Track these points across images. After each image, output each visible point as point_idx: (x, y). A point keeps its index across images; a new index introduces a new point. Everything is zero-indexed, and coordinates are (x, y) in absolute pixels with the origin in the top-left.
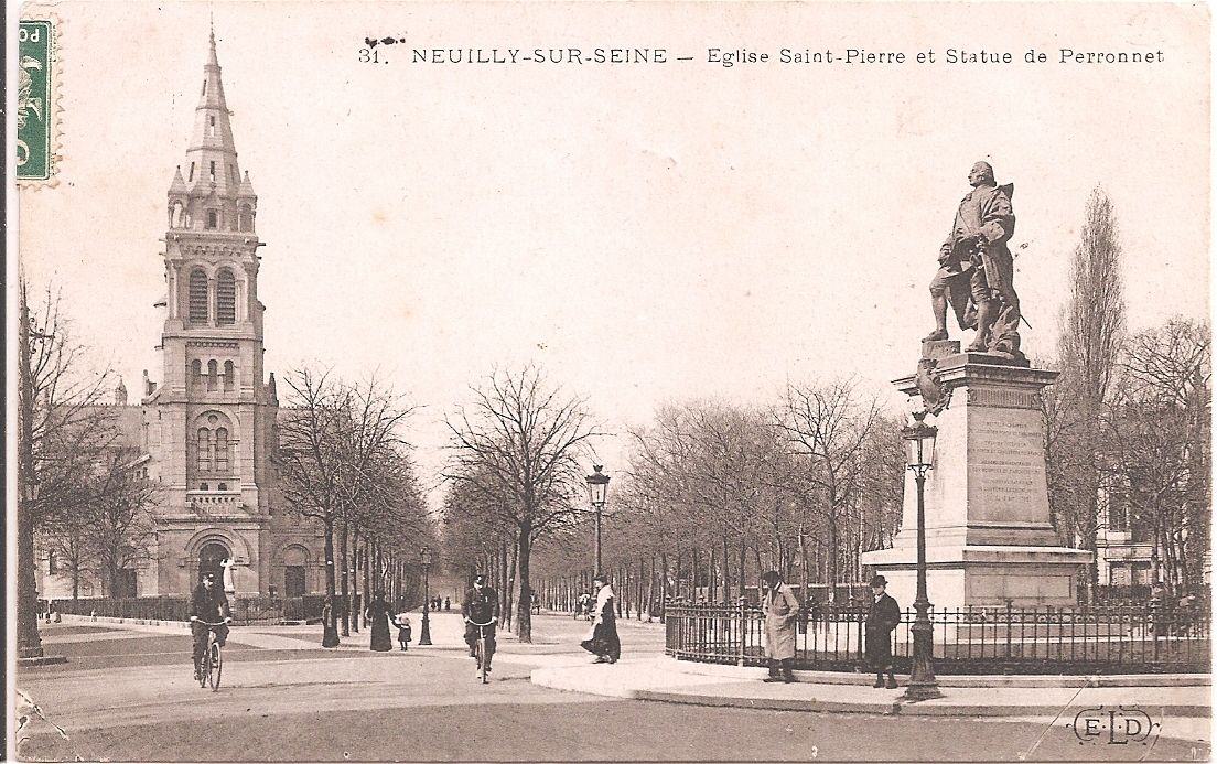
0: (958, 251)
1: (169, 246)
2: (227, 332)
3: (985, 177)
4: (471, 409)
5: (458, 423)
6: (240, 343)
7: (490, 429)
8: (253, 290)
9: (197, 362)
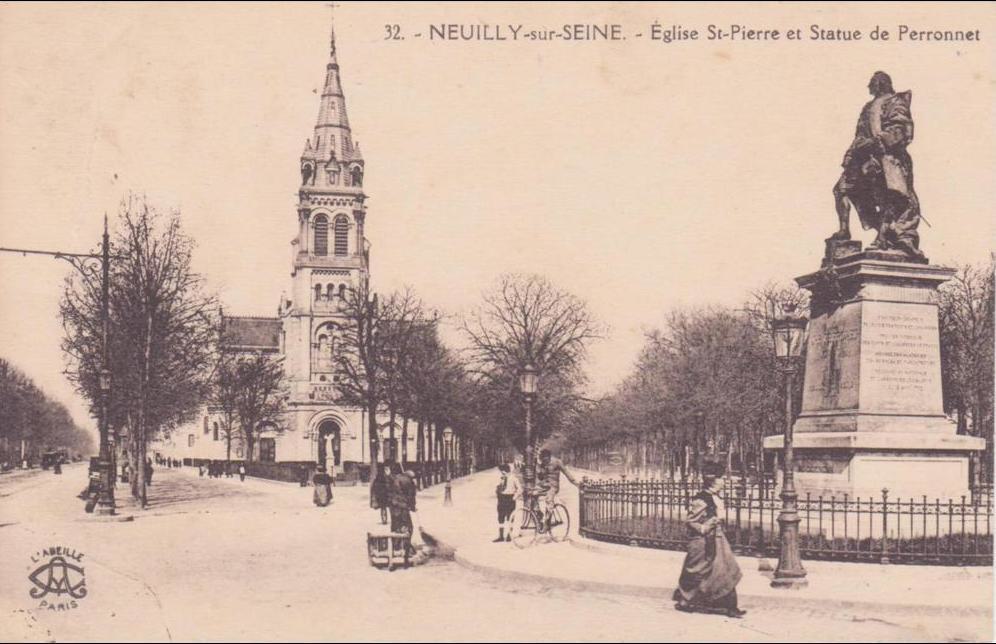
0: (857, 158)
1: (301, 199)
2: (341, 262)
3: (880, 84)
4: (485, 318)
5: (475, 328)
6: (352, 272)
7: (502, 333)
8: (360, 232)
9: (318, 287)
